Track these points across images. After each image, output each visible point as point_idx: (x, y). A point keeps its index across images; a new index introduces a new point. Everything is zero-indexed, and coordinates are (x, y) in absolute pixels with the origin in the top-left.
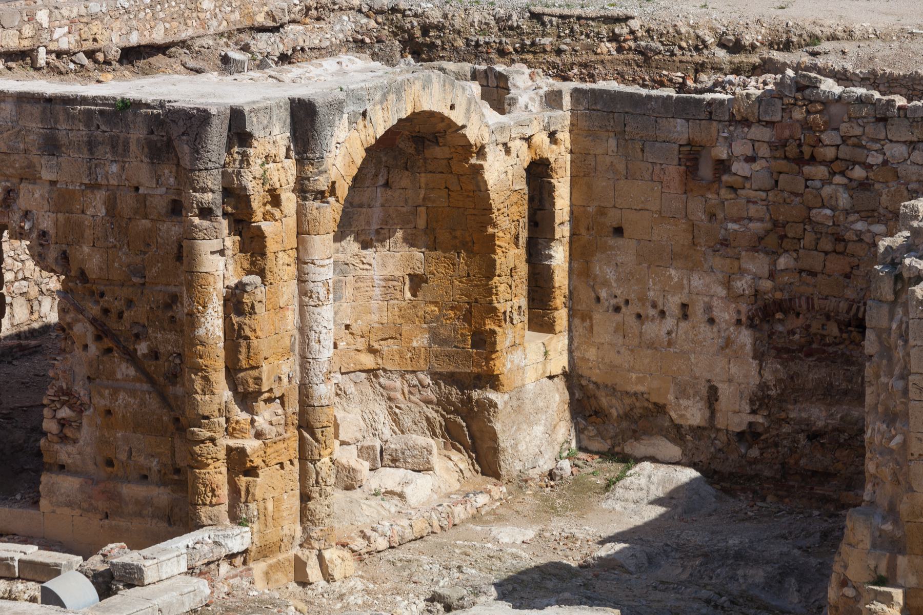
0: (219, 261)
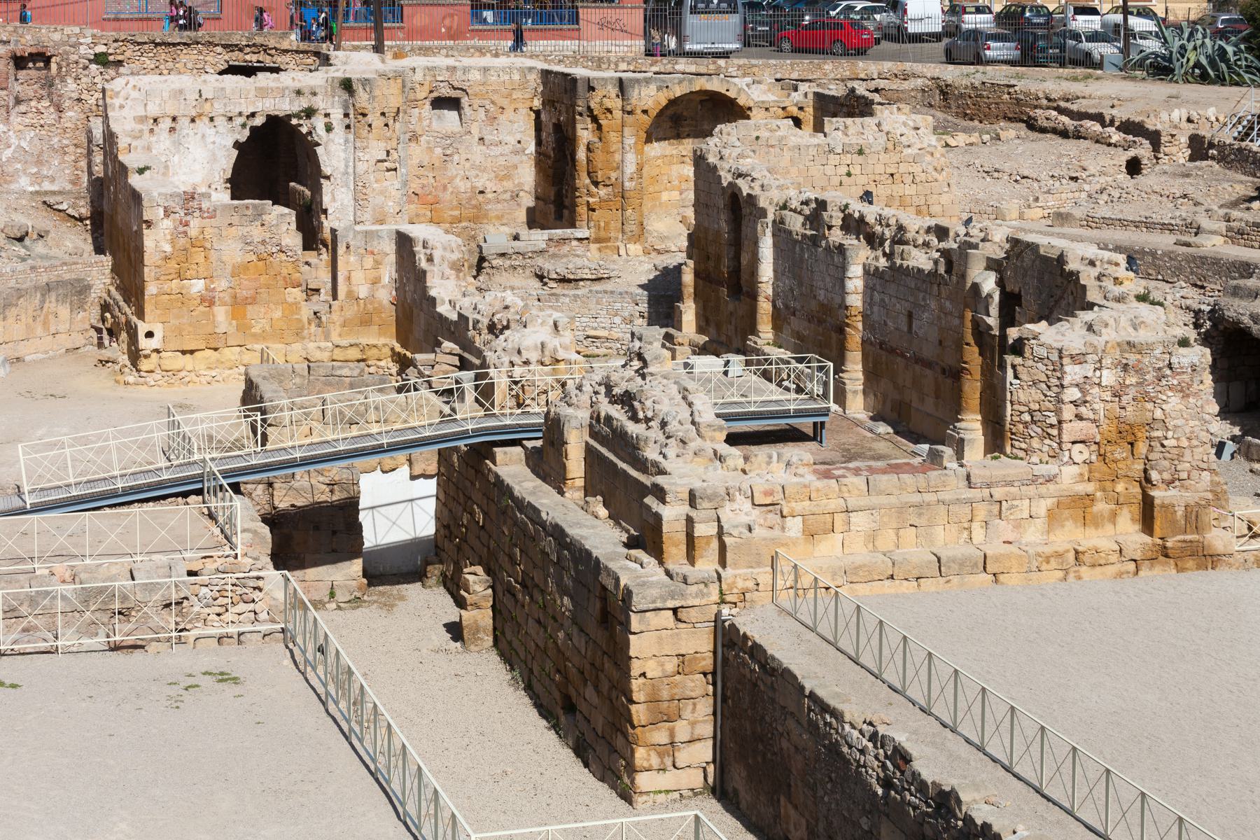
0: (585, 132)
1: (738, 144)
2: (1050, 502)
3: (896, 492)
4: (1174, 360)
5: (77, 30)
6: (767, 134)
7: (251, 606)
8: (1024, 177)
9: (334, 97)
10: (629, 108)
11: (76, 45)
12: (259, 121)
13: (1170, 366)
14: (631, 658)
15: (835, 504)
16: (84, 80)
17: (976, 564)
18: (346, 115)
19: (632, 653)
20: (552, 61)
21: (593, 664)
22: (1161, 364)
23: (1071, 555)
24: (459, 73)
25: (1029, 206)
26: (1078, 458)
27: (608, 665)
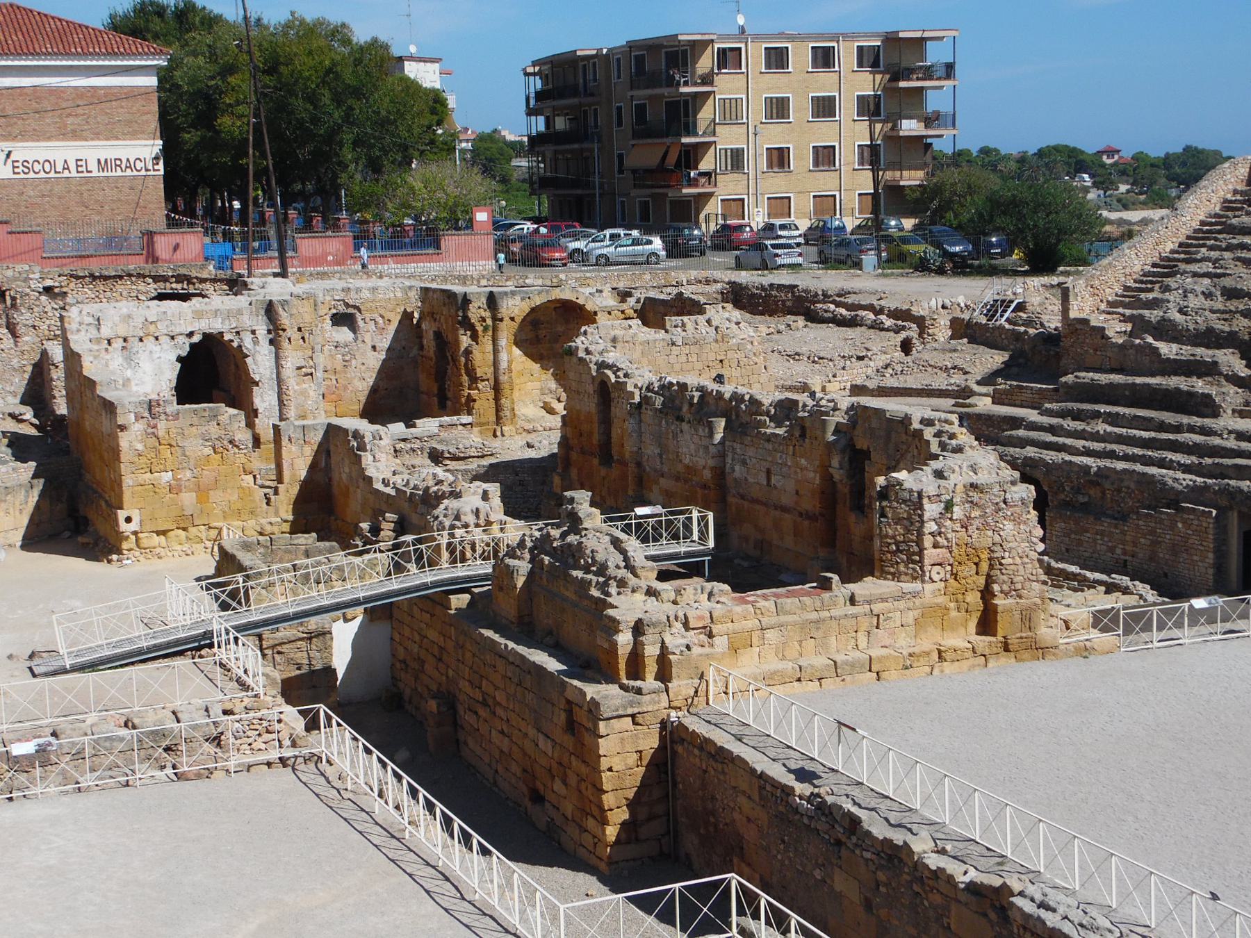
1: (601, 341)
2: (917, 613)
3: (798, 611)
4: (1008, 496)
5: (27, 267)
6: (622, 332)
7: (275, 736)
8: (820, 358)
9: (258, 316)
10: (500, 316)
11: (27, 279)
12: (196, 339)
13: (1005, 502)
14: (601, 756)
15: (752, 623)
16: (36, 309)
17: (863, 666)
18: (269, 332)
19: (601, 752)
20: (426, 279)
21: (560, 764)
22: (998, 500)
23: (935, 656)
24: (353, 293)
25: (830, 381)
26: (935, 577)
27: (575, 762)
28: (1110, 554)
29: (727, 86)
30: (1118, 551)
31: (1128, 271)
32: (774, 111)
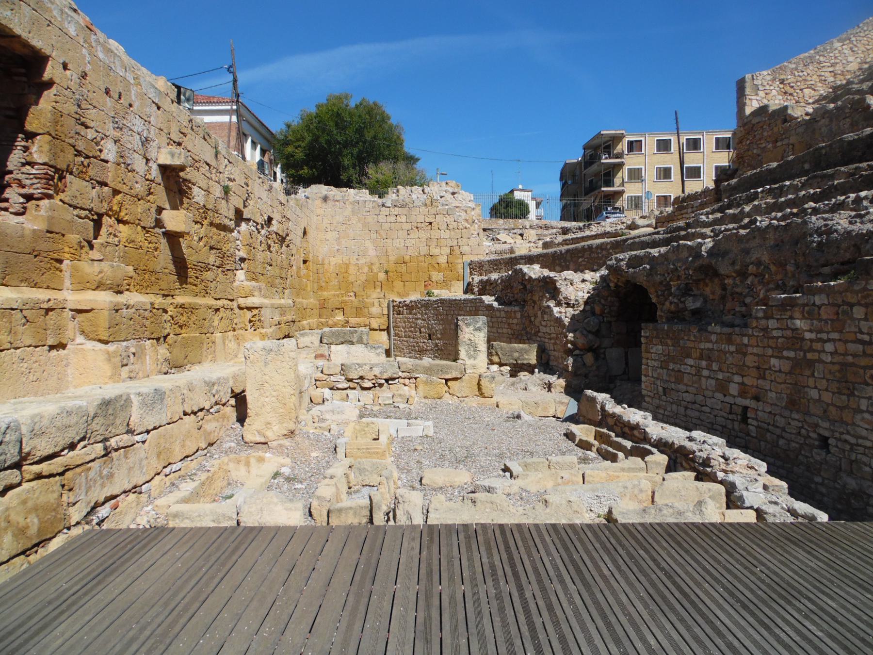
28: (719, 396)
29: (631, 162)
30: (734, 389)
31: (839, 68)
32: (662, 175)
